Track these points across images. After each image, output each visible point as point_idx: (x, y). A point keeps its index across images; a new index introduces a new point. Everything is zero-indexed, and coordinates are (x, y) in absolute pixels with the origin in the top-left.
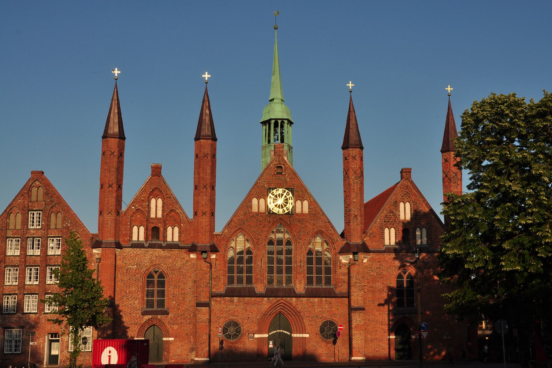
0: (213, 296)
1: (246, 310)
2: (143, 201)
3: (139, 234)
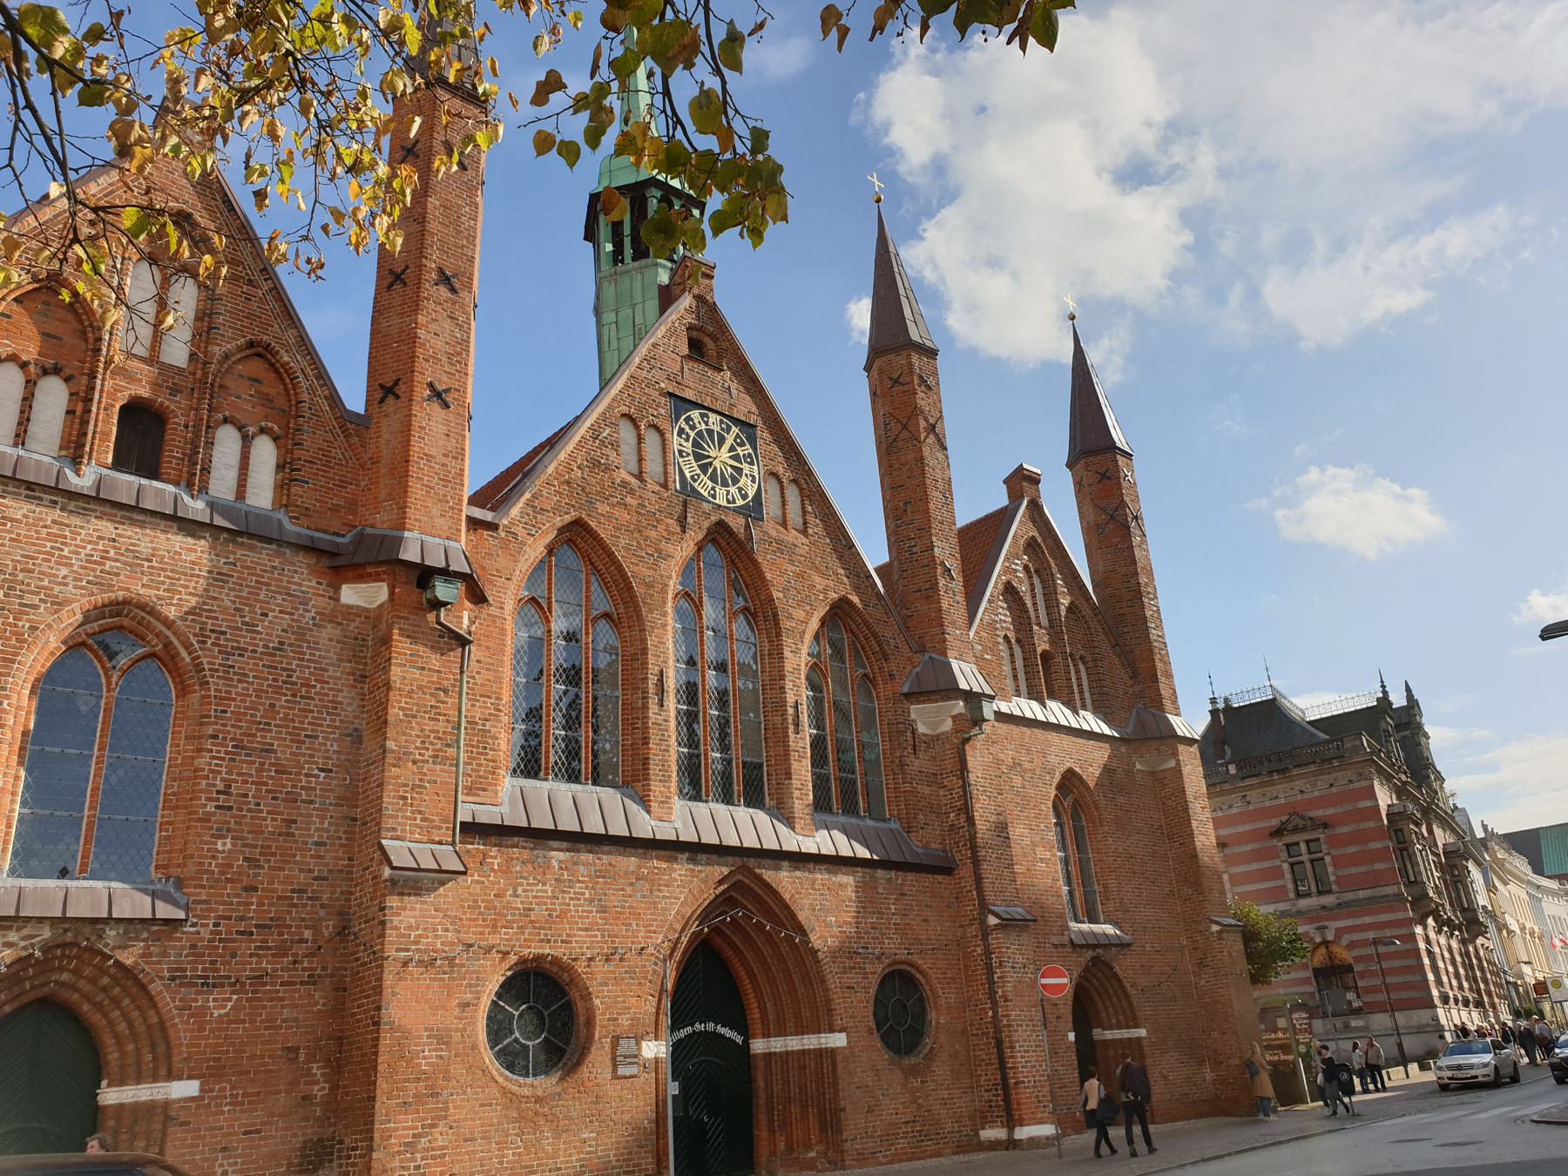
1: (603, 910)
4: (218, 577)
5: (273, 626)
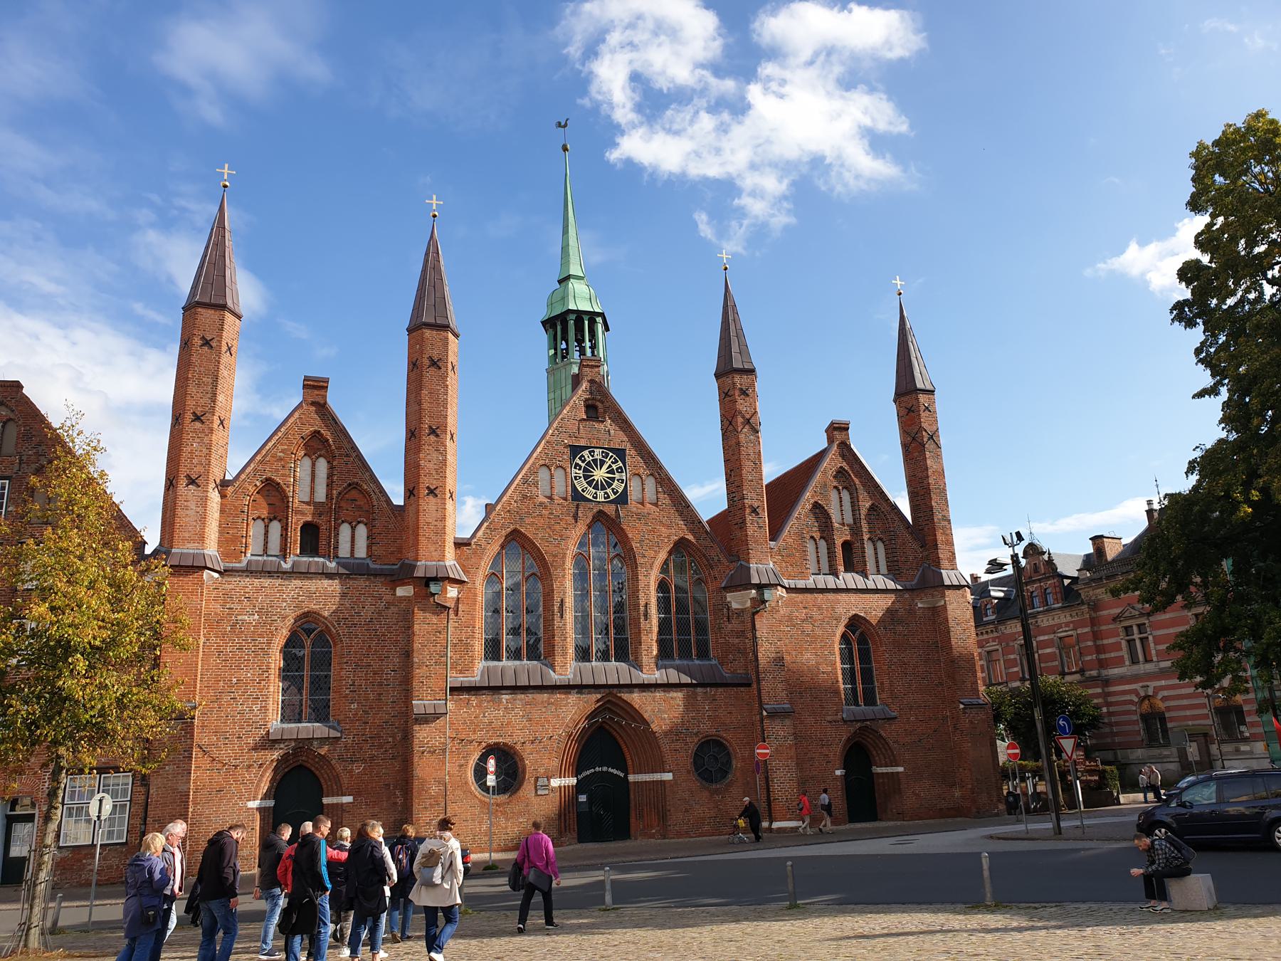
2: (281, 459)
4: (343, 595)
5: (368, 612)
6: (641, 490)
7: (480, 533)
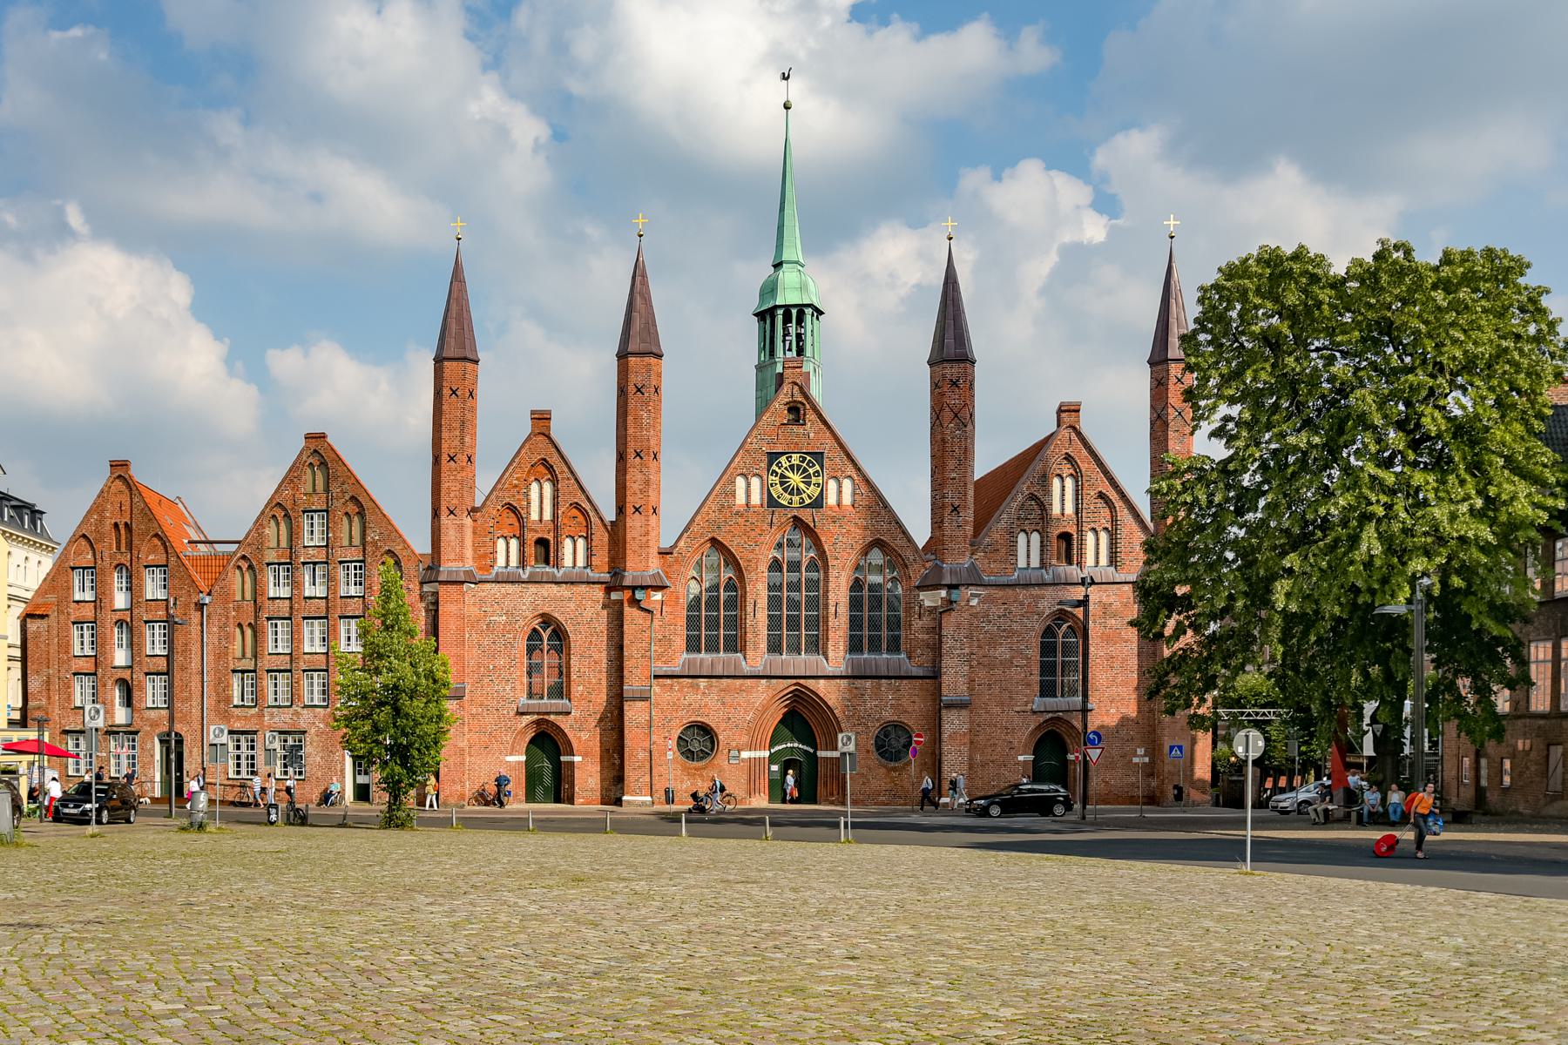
0: (656, 677)
3: (506, 553)
6: (840, 493)
7: (682, 544)
